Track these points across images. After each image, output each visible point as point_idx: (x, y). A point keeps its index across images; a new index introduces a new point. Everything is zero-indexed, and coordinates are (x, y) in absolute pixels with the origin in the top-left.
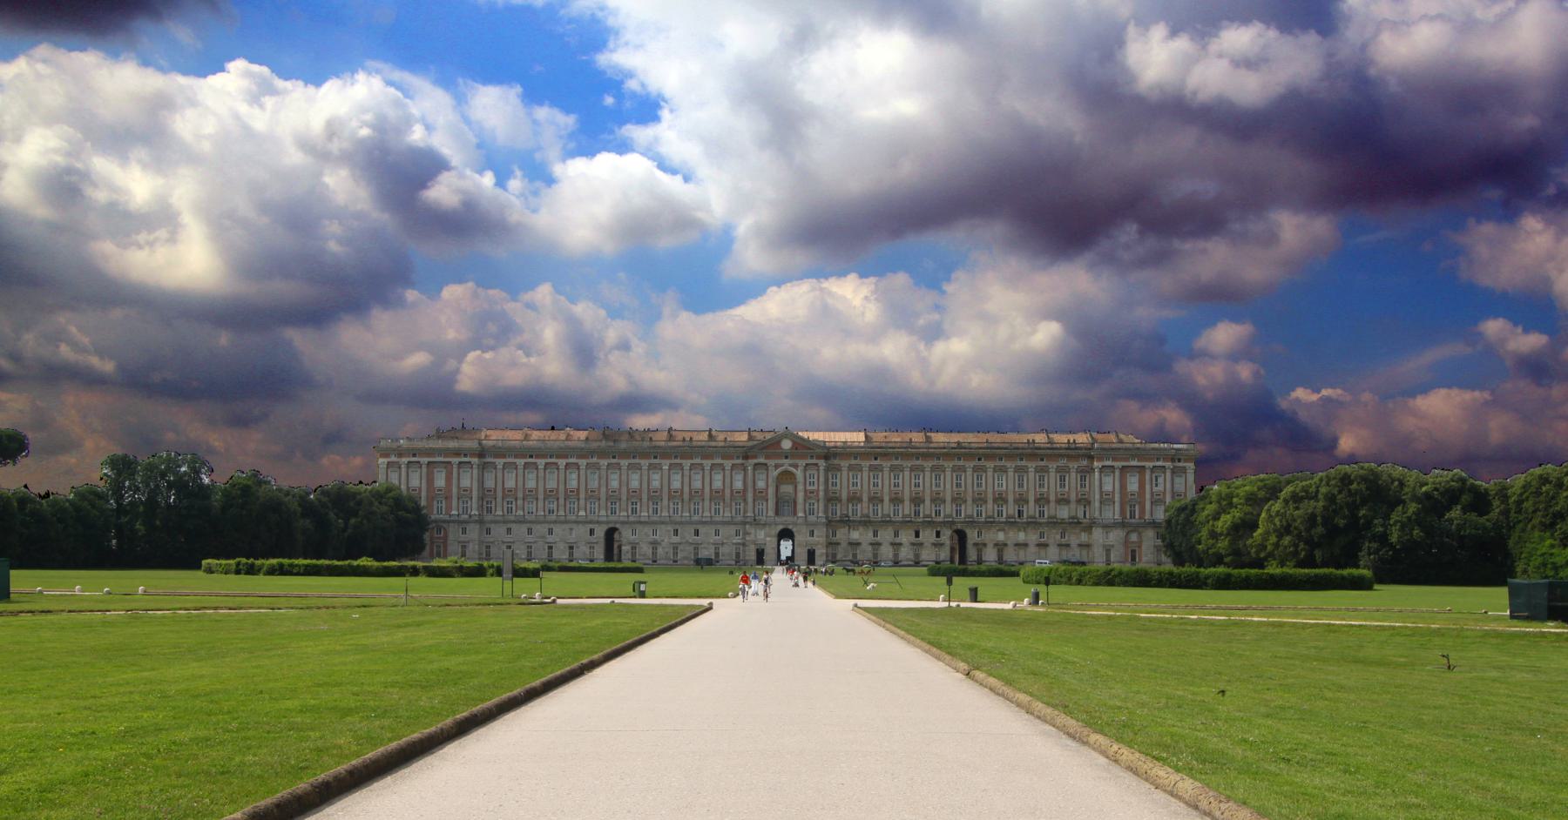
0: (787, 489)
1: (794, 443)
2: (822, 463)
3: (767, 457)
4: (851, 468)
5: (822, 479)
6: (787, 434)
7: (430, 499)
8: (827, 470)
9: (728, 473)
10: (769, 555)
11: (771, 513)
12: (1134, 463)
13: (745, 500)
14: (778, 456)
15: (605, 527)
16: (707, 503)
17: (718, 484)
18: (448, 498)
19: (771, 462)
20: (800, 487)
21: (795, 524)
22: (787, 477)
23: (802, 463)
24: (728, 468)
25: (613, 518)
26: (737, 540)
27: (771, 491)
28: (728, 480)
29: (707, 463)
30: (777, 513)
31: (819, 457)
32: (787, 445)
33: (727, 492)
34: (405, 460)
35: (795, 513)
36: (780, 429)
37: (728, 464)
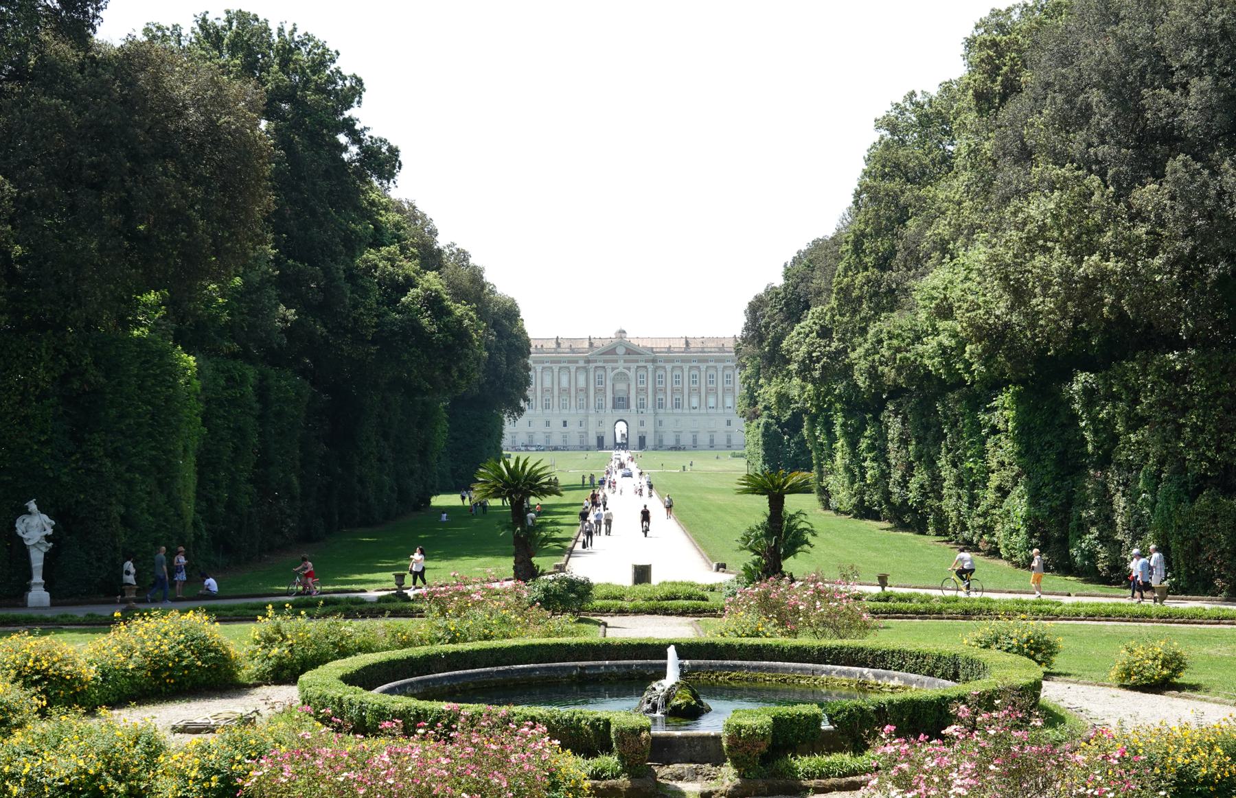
0: (621, 386)
2: (650, 366)
3: (605, 361)
9: (573, 374)
10: (608, 441)
14: (616, 361)
16: (556, 399)
20: (633, 386)
24: (573, 370)
26: (582, 429)
31: (646, 361)
35: (628, 407)
37: (573, 367)
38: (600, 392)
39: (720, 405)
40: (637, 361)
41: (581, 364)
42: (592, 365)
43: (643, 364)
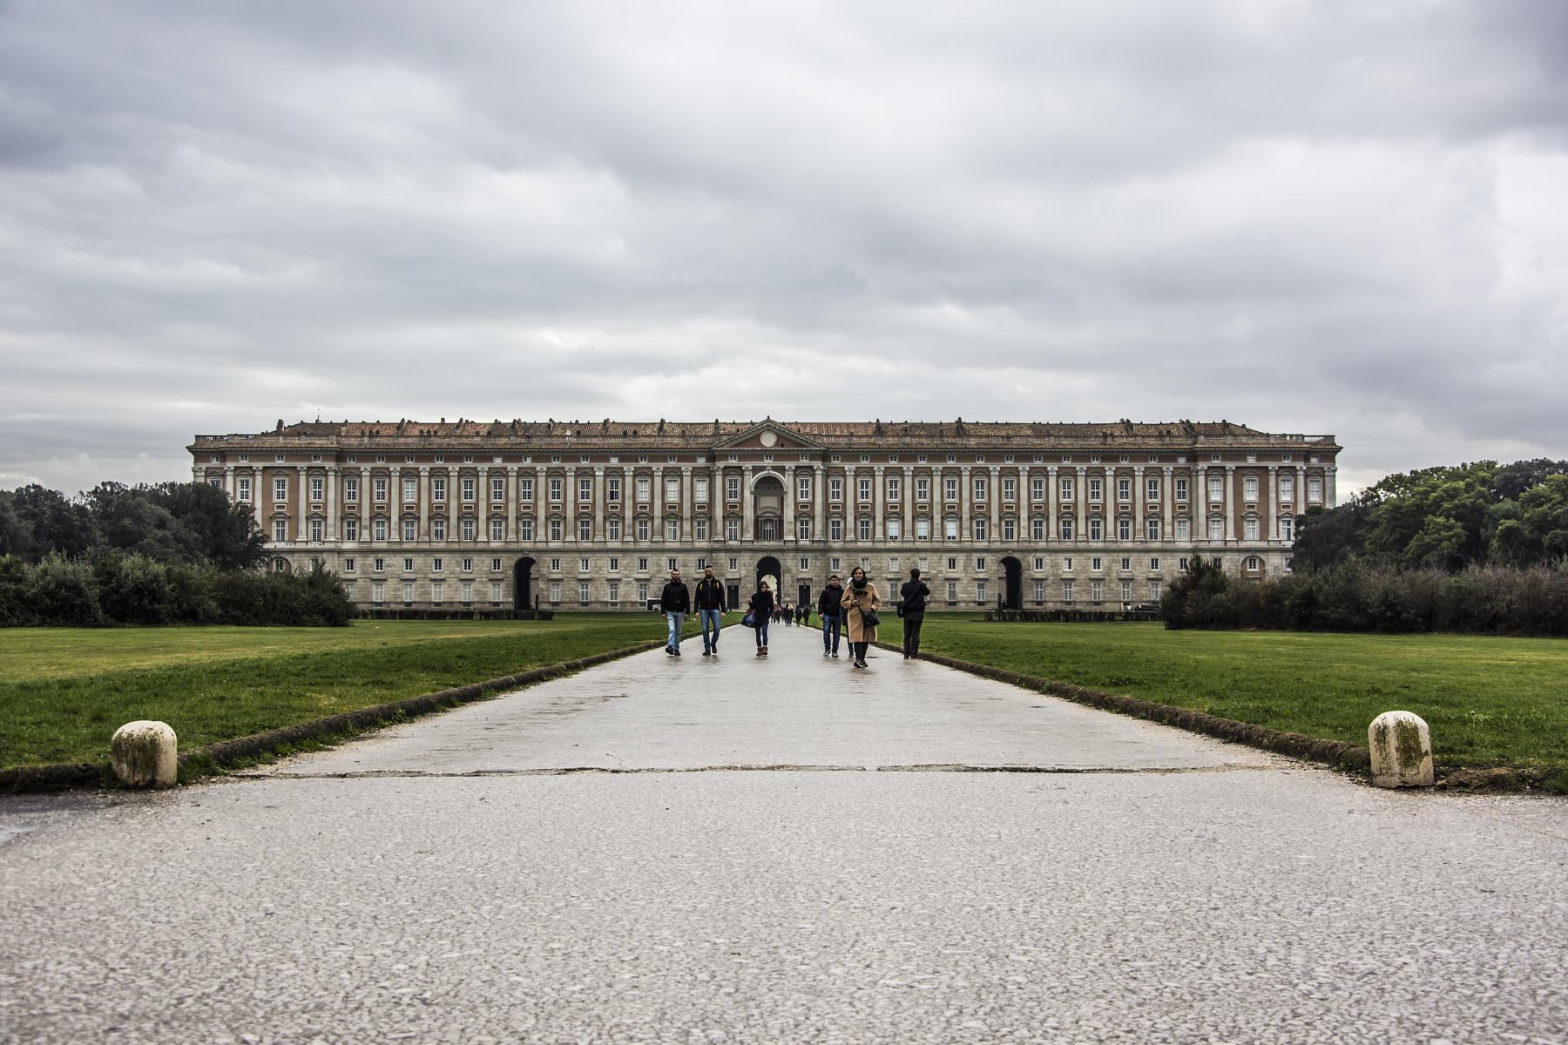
0: (769, 502)
1: (779, 436)
2: (817, 464)
3: (743, 457)
4: (858, 473)
6: (769, 425)
7: (269, 519)
8: (826, 475)
11: (749, 536)
12: (1251, 461)
13: (711, 518)
15: (516, 558)
17: (672, 497)
18: (293, 519)
19: (748, 465)
20: (789, 500)
21: (782, 551)
22: (769, 485)
23: (790, 465)
25: (528, 545)
28: (687, 494)
29: (658, 467)
30: (757, 536)
32: (768, 441)
33: (687, 505)
34: (231, 465)
35: (780, 536)
36: (759, 419)
37: (686, 467)
38: (733, 514)
39: (937, 535)
40: (795, 457)
41: (701, 462)
42: (721, 464)
43: (804, 462)
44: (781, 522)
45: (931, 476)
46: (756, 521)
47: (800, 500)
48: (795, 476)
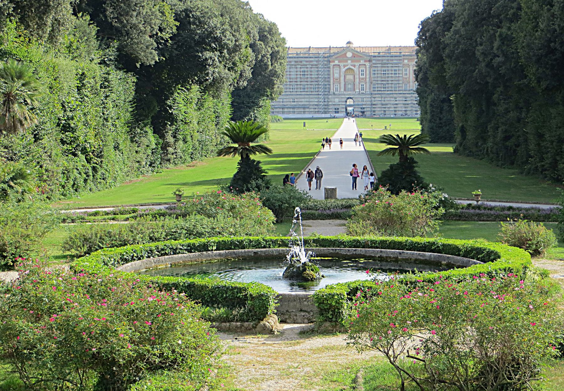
0: (350, 77)
1: (353, 54)
2: (368, 64)
5: (368, 72)
8: (371, 67)
11: (342, 90)
19: (342, 64)
20: (357, 76)
23: (357, 64)
27: (342, 78)
30: (345, 90)
32: (349, 55)
35: (354, 90)
43: (362, 62)
44: (354, 84)
45: (409, 67)
46: (345, 84)
47: (361, 77)
48: (359, 68)
